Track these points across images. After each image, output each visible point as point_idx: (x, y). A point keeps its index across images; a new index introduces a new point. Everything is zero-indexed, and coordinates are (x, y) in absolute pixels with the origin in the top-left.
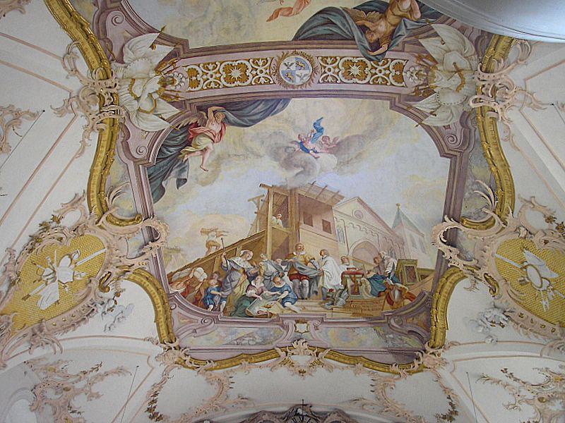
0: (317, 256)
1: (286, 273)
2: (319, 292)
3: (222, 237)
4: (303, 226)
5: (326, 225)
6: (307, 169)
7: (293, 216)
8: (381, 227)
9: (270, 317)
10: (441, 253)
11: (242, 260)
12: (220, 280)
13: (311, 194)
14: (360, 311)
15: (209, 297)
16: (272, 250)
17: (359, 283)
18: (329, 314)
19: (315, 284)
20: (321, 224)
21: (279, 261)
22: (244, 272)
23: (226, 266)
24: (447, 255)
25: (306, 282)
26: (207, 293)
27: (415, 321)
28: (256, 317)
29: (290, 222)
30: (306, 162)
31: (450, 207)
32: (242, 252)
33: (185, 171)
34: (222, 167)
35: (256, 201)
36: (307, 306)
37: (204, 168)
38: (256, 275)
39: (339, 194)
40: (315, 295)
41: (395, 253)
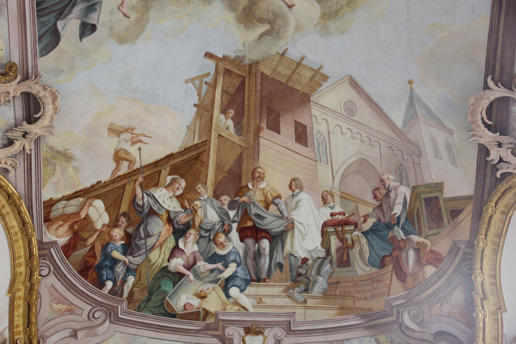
0: (285, 191)
1: (235, 226)
2: (286, 268)
3: (139, 145)
4: (266, 133)
5: (300, 130)
6: (276, 27)
7: (252, 114)
8: (385, 130)
9: (204, 320)
10: (484, 151)
11: (168, 196)
12: (130, 230)
13: (279, 74)
14: (349, 303)
15: (108, 263)
16: (216, 177)
17: (349, 242)
18: (300, 314)
19: (280, 249)
20: (292, 129)
21: (226, 199)
22: (170, 221)
23: (140, 203)
24: (494, 155)
25: (265, 243)
26: (107, 256)
27: (446, 308)
28: (183, 317)
29: (245, 126)
30: (274, 14)
31: (494, 67)
32: (169, 178)
33: (96, 10)
34: (152, 14)
35: (197, 83)
36: (265, 296)
37: (125, 10)
38: (188, 226)
39: (322, 71)
40: (278, 269)
41: (406, 175)
